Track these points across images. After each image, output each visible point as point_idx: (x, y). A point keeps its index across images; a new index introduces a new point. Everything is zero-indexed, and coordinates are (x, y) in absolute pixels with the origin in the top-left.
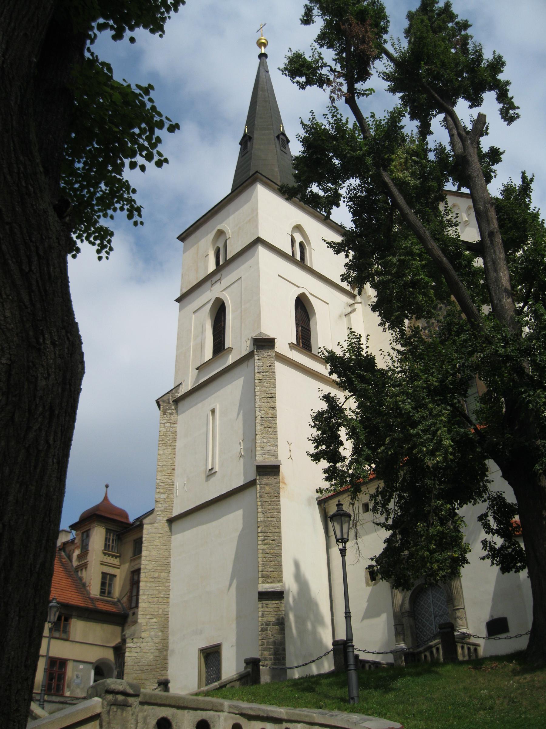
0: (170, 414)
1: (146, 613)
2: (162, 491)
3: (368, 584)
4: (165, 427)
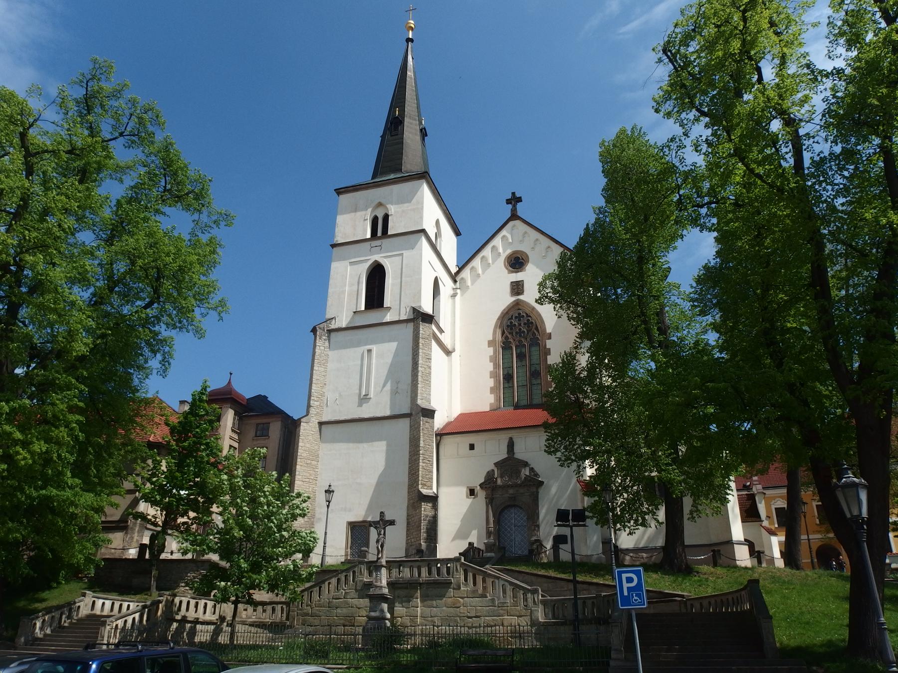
3: (467, 497)
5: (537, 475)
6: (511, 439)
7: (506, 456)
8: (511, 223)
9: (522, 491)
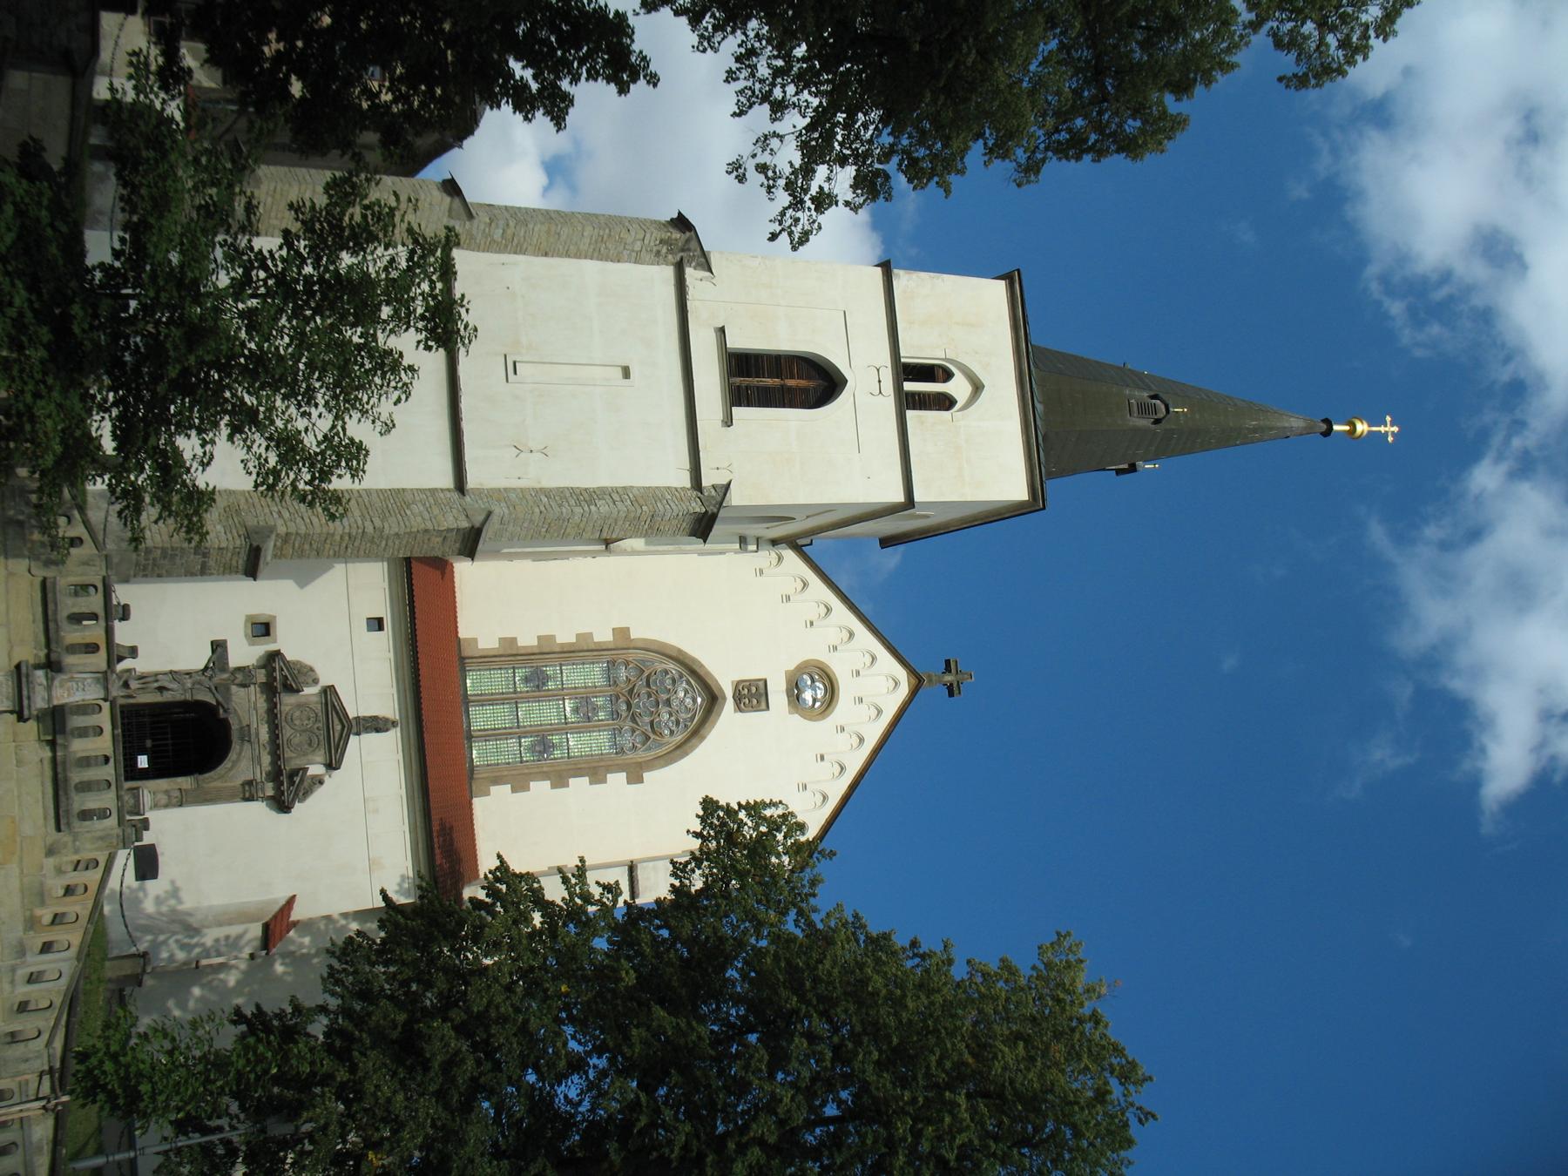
0: (658, 253)
1: (278, 196)
2: (509, 232)
3: (249, 618)
4: (635, 240)
5: (307, 794)
6: (394, 724)
7: (352, 714)
8: (901, 674)
9: (266, 759)
